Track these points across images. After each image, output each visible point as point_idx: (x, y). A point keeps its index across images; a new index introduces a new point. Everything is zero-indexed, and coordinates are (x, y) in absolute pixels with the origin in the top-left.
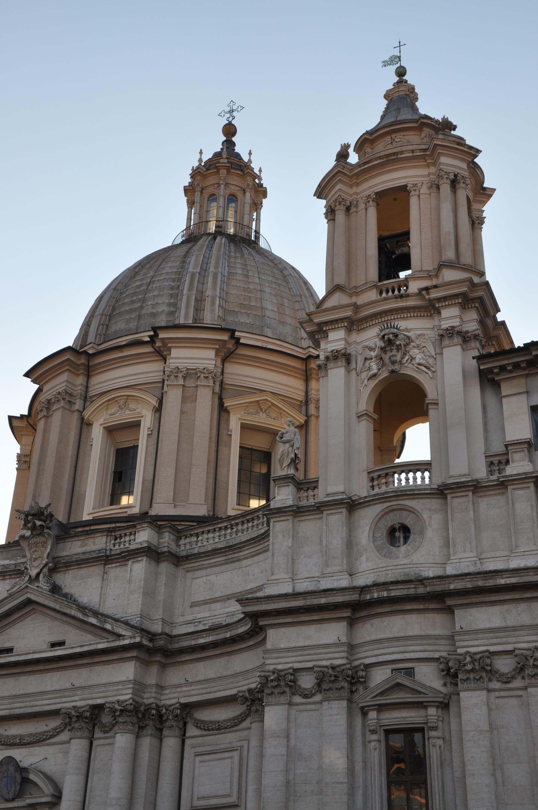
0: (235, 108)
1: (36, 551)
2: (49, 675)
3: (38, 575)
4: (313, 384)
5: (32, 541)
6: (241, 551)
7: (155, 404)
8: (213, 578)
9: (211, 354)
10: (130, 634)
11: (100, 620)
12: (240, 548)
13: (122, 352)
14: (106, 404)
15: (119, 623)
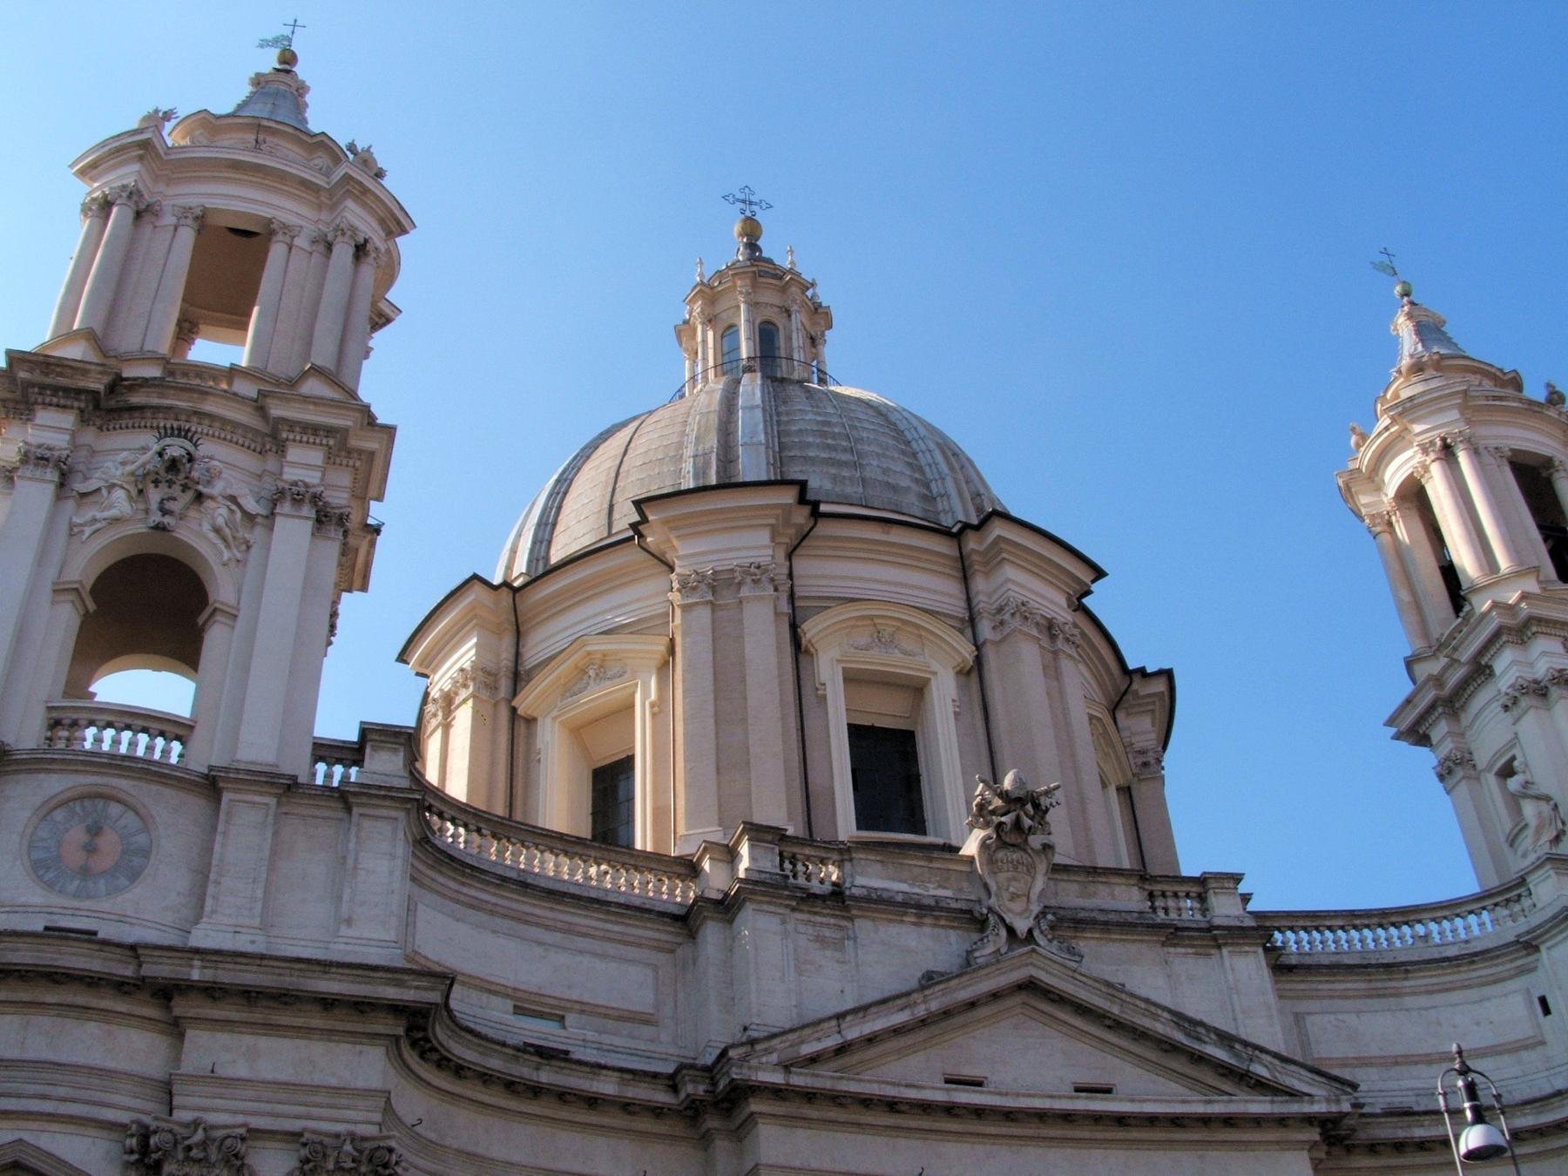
0: (753, 199)
1: (1014, 879)
2: (1097, 1153)
3: (1030, 931)
4: (1120, 715)
5: (1001, 855)
6: (1406, 979)
7: (967, 656)
8: (1352, 1019)
9: (1063, 602)
10: (1324, 1093)
11: (1237, 1055)
12: (1407, 971)
13: (888, 533)
14: (853, 622)
15: (1293, 1068)
